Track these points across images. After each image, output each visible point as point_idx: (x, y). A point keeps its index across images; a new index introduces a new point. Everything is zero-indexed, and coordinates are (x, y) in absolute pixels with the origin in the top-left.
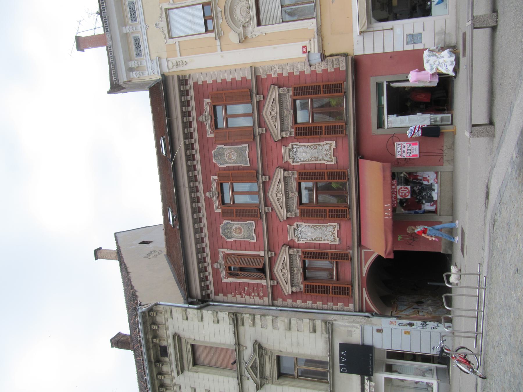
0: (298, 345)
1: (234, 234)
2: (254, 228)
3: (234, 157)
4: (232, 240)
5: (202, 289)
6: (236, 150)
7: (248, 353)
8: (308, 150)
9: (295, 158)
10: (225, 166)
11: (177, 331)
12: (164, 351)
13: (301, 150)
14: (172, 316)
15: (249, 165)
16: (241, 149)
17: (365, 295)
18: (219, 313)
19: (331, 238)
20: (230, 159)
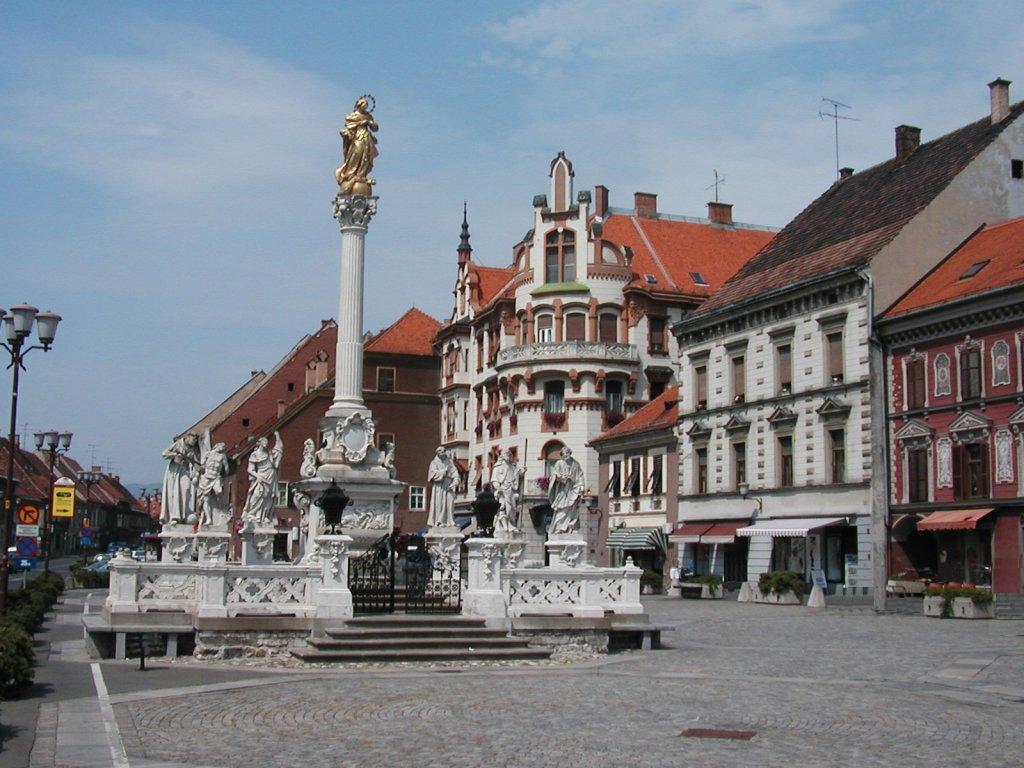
0: (853, 451)
1: (940, 370)
2: (946, 394)
3: (1000, 368)
4: (935, 368)
5: (892, 335)
6: (1005, 370)
7: (843, 399)
8: (1006, 452)
9: (1000, 439)
10: (993, 356)
11: (849, 315)
12: (833, 300)
13: (1007, 446)
14: (860, 307)
15: (993, 385)
16: (1006, 376)
17: (904, 516)
18: (868, 364)
19: (942, 480)
20: (999, 362)
